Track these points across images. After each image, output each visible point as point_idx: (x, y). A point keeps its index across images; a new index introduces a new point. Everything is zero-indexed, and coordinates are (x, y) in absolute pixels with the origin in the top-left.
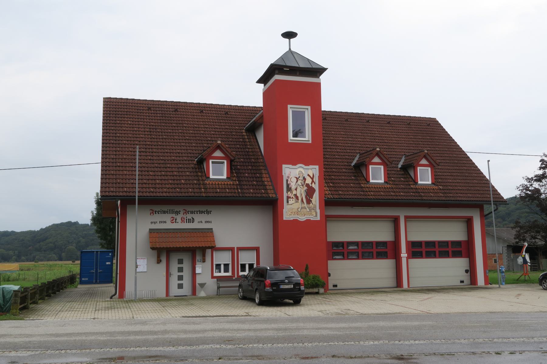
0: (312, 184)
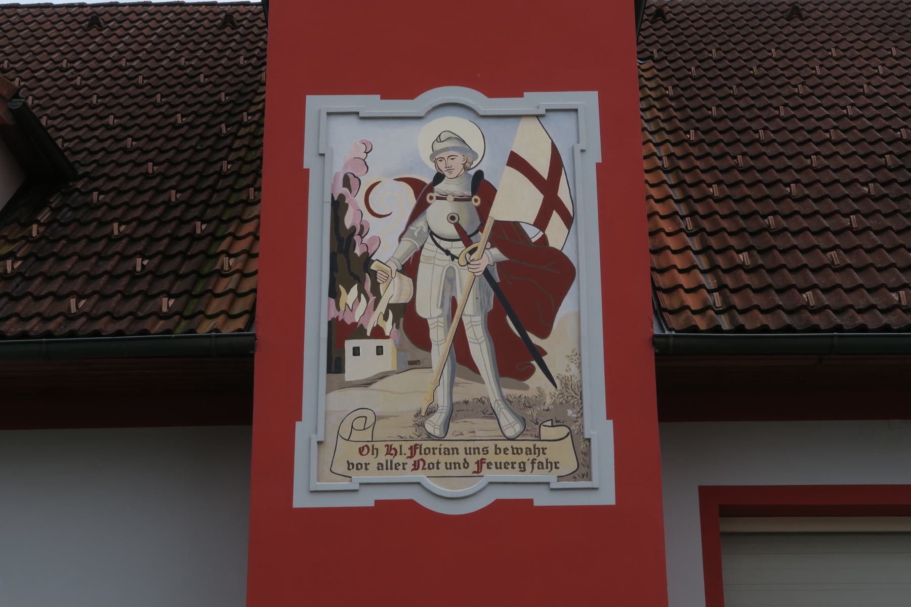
0: (541, 222)
